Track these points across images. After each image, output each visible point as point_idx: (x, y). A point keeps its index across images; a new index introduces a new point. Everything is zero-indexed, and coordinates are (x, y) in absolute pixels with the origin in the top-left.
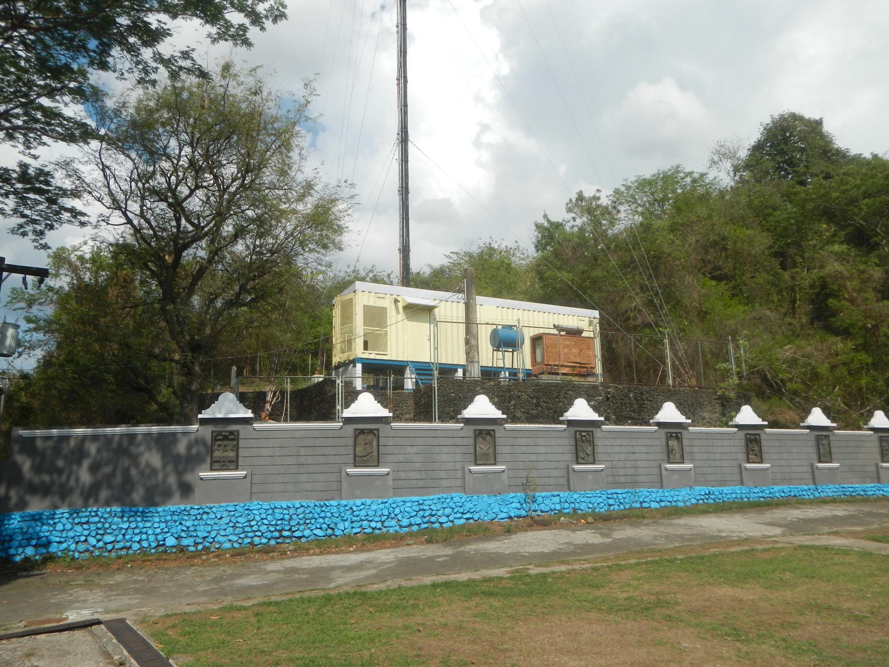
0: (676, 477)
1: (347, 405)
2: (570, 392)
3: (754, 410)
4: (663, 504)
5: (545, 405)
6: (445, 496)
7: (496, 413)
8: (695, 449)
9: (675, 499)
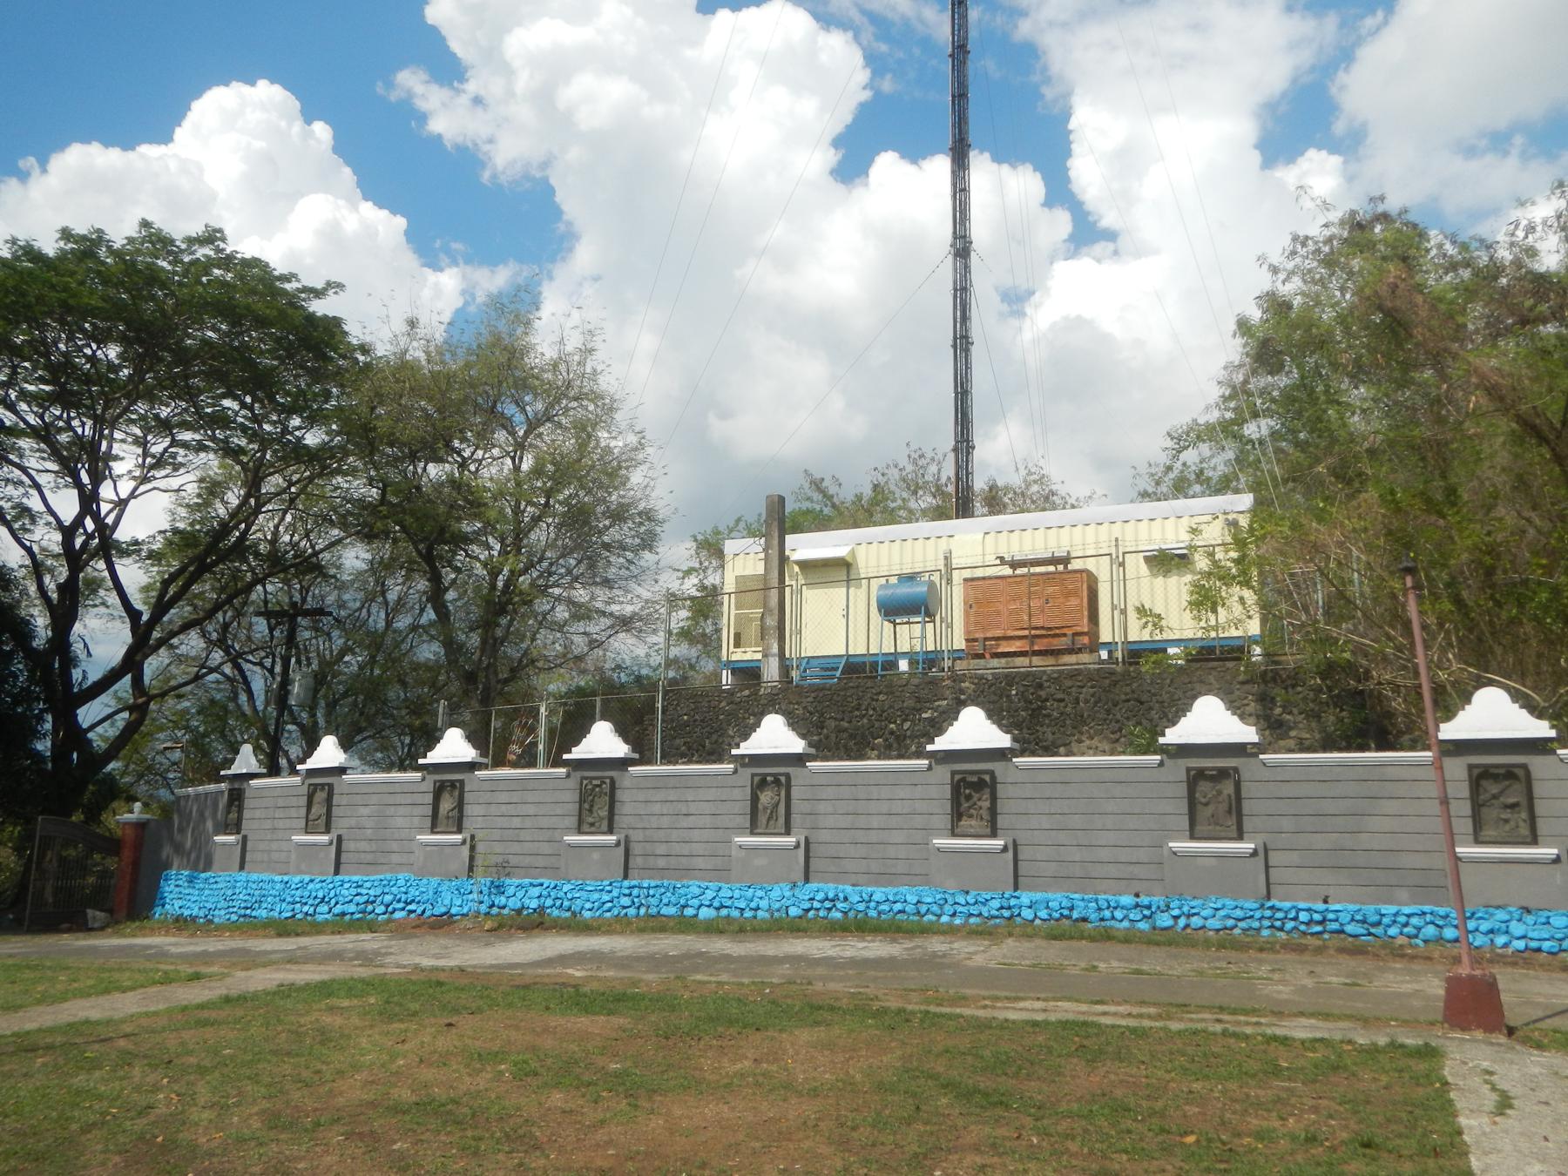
0: (760, 861)
1: (1449, 714)
2: (881, 697)
3: (990, 716)
4: (724, 912)
5: (833, 724)
6: (388, 876)
7: (1000, 739)
8: (822, 807)
9: (753, 905)
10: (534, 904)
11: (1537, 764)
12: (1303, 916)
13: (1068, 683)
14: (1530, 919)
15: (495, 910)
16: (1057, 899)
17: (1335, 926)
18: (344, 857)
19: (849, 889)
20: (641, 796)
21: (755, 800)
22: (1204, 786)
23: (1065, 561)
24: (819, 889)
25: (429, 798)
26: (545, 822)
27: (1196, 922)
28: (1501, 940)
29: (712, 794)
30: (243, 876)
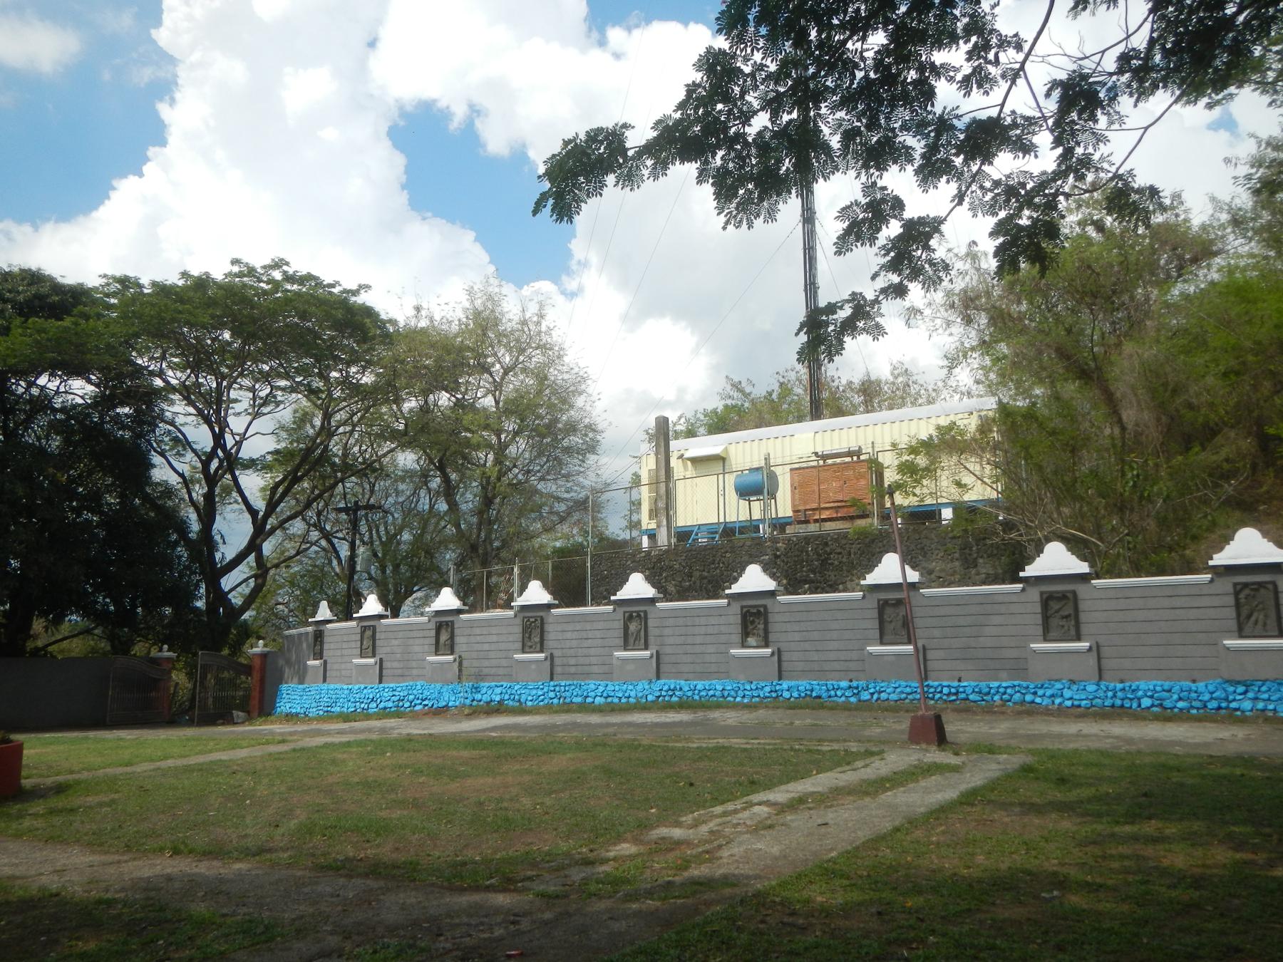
4: (609, 700)
8: (667, 631)
10: (498, 698)
11: (1081, 589)
12: (946, 690)
13: (844, 542)
14: (1075, 687)
15: (475, 703)
16: (803, 684)
17: (963, 696)
18: (384, 672)
19: (683, 682)
20: (560, 628)
21: (626, 628)
22: (889, 611)
23: (858, 453)
24: (666, 683)
25: (433, 633)
26: (503, 646)
27: (884, 696)
28: (1058, 701)
29: (601, 625)
30: (325, 686)
